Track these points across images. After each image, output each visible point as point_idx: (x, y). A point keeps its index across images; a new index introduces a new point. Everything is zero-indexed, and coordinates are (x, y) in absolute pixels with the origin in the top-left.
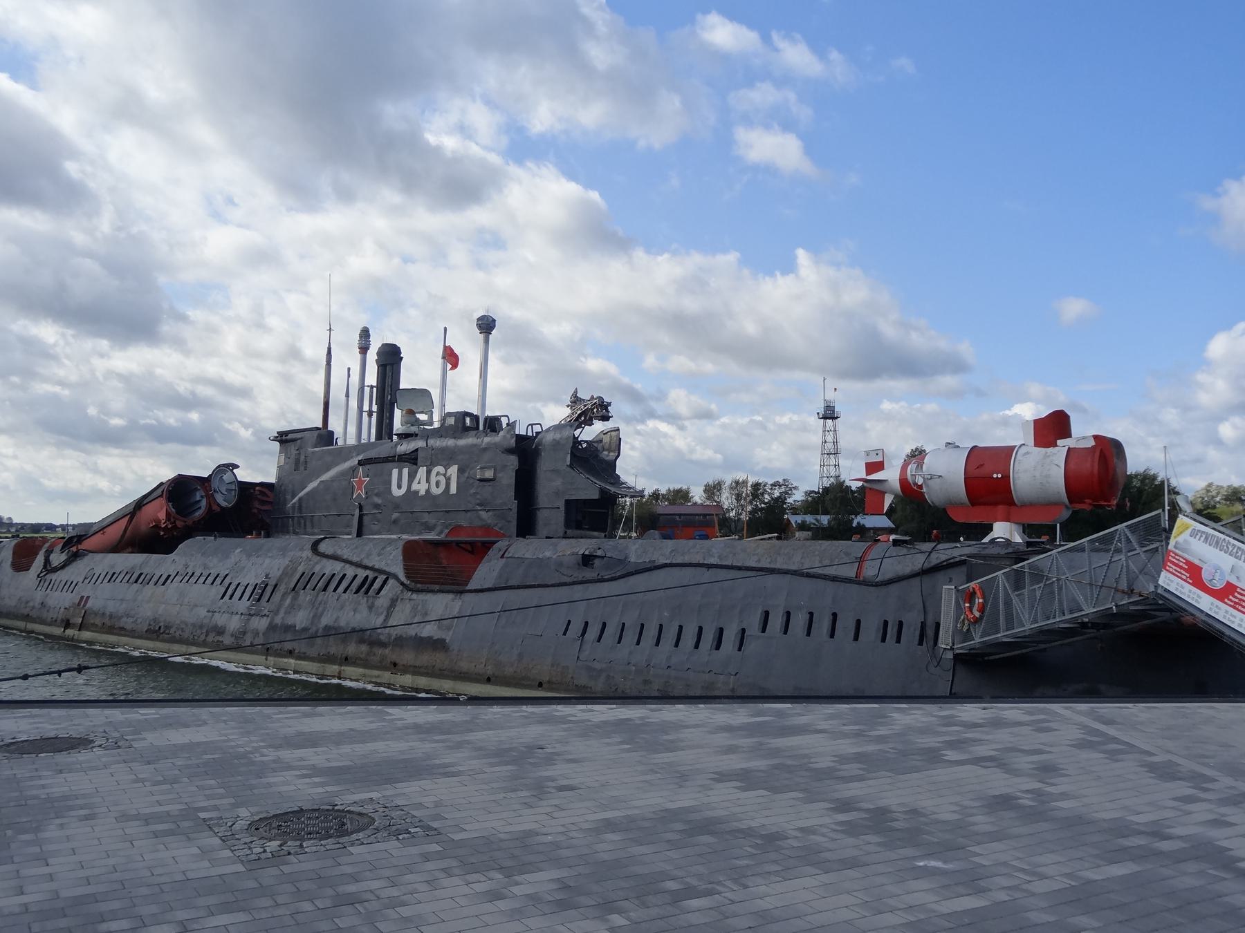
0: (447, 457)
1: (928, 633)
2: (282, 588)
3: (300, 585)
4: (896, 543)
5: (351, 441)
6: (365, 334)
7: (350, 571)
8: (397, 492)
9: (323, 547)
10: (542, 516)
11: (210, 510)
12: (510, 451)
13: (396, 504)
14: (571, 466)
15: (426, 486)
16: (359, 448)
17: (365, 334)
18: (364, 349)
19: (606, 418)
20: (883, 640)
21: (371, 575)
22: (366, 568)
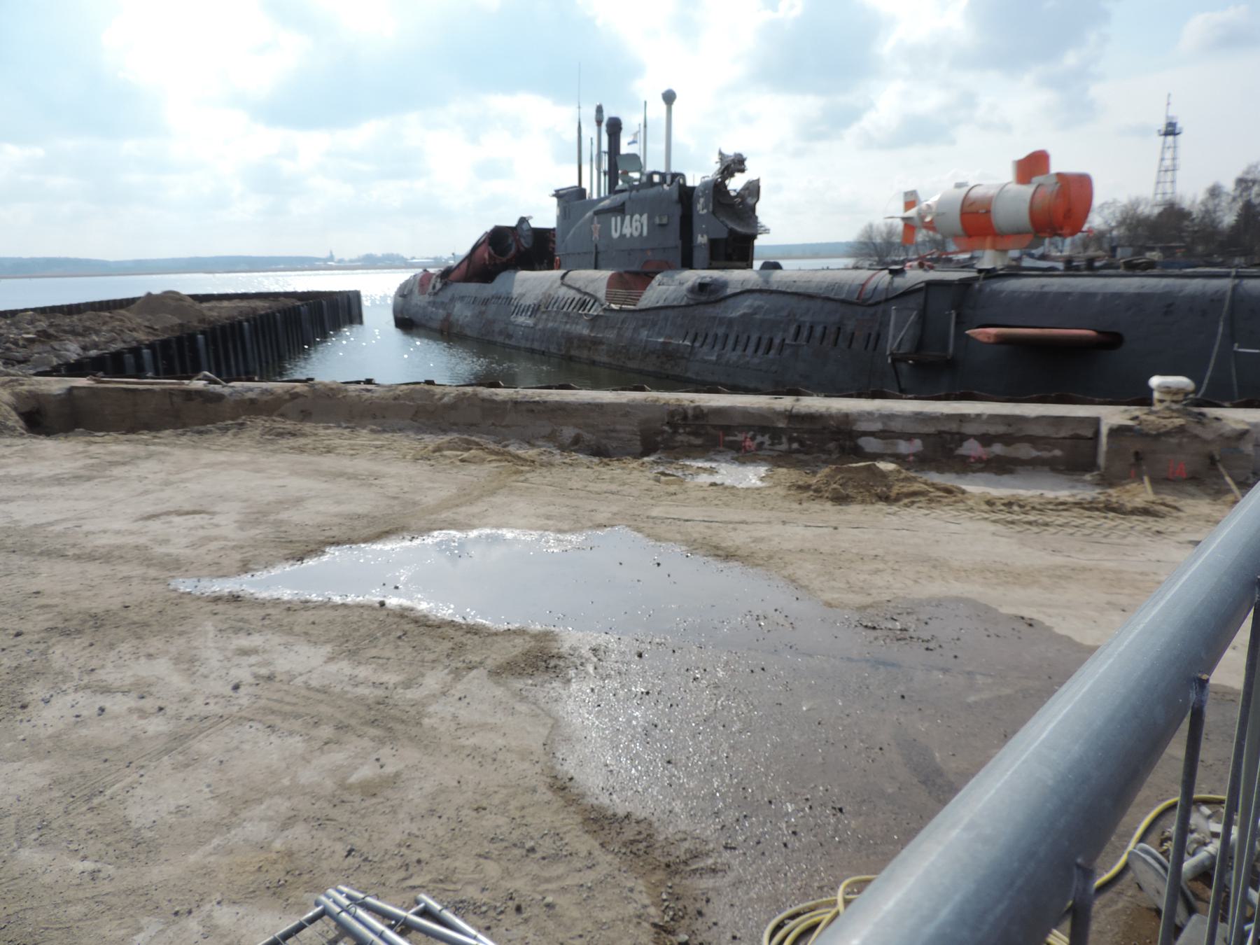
5: (595, 196)
6: (599, 110)
7: (578, 296)
8: (615, 235)
11: (518, 250)
16: (600, 200)
17: (599, 110)
18: (599, 122)
19: (742, 171)
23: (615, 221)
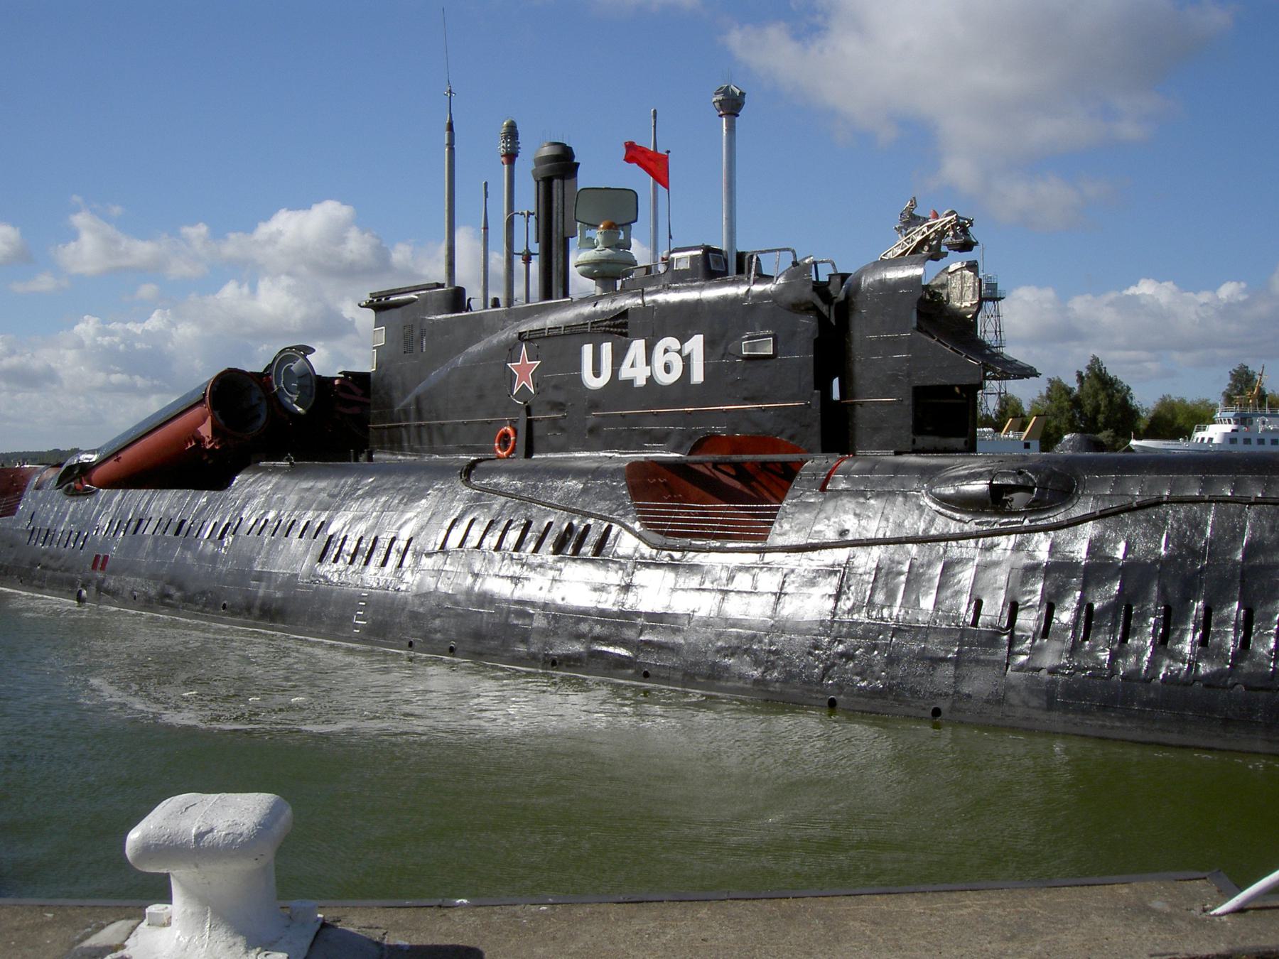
0: (680, 321)
6: (512, 133)
12: (800, 308)
13: (596, 400)
14: (919, 328)
15: (647, 371)
17: (512, 133)
18: (511, 157)
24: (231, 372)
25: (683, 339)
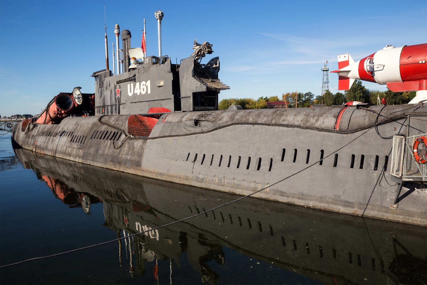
1: (382, 163)
2: (88, 137)
3: (94, 136)
4: (358, 107)
8: (130, 94)
9: (104, 120)
10: (183, 102)
19: (210, 52)
20: (352, 166)
21: (116, 131)
22: (115, 128)
23: (130, 86)
24: (61, 94)
25: (146, 82)
